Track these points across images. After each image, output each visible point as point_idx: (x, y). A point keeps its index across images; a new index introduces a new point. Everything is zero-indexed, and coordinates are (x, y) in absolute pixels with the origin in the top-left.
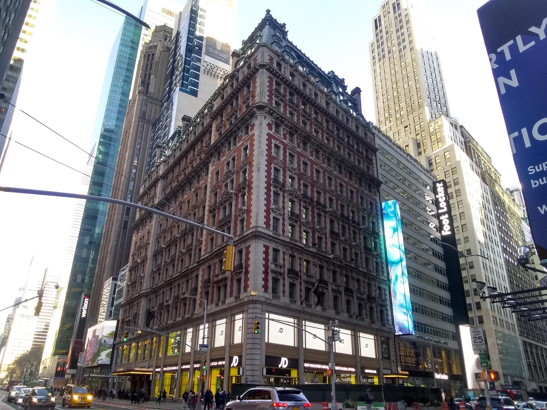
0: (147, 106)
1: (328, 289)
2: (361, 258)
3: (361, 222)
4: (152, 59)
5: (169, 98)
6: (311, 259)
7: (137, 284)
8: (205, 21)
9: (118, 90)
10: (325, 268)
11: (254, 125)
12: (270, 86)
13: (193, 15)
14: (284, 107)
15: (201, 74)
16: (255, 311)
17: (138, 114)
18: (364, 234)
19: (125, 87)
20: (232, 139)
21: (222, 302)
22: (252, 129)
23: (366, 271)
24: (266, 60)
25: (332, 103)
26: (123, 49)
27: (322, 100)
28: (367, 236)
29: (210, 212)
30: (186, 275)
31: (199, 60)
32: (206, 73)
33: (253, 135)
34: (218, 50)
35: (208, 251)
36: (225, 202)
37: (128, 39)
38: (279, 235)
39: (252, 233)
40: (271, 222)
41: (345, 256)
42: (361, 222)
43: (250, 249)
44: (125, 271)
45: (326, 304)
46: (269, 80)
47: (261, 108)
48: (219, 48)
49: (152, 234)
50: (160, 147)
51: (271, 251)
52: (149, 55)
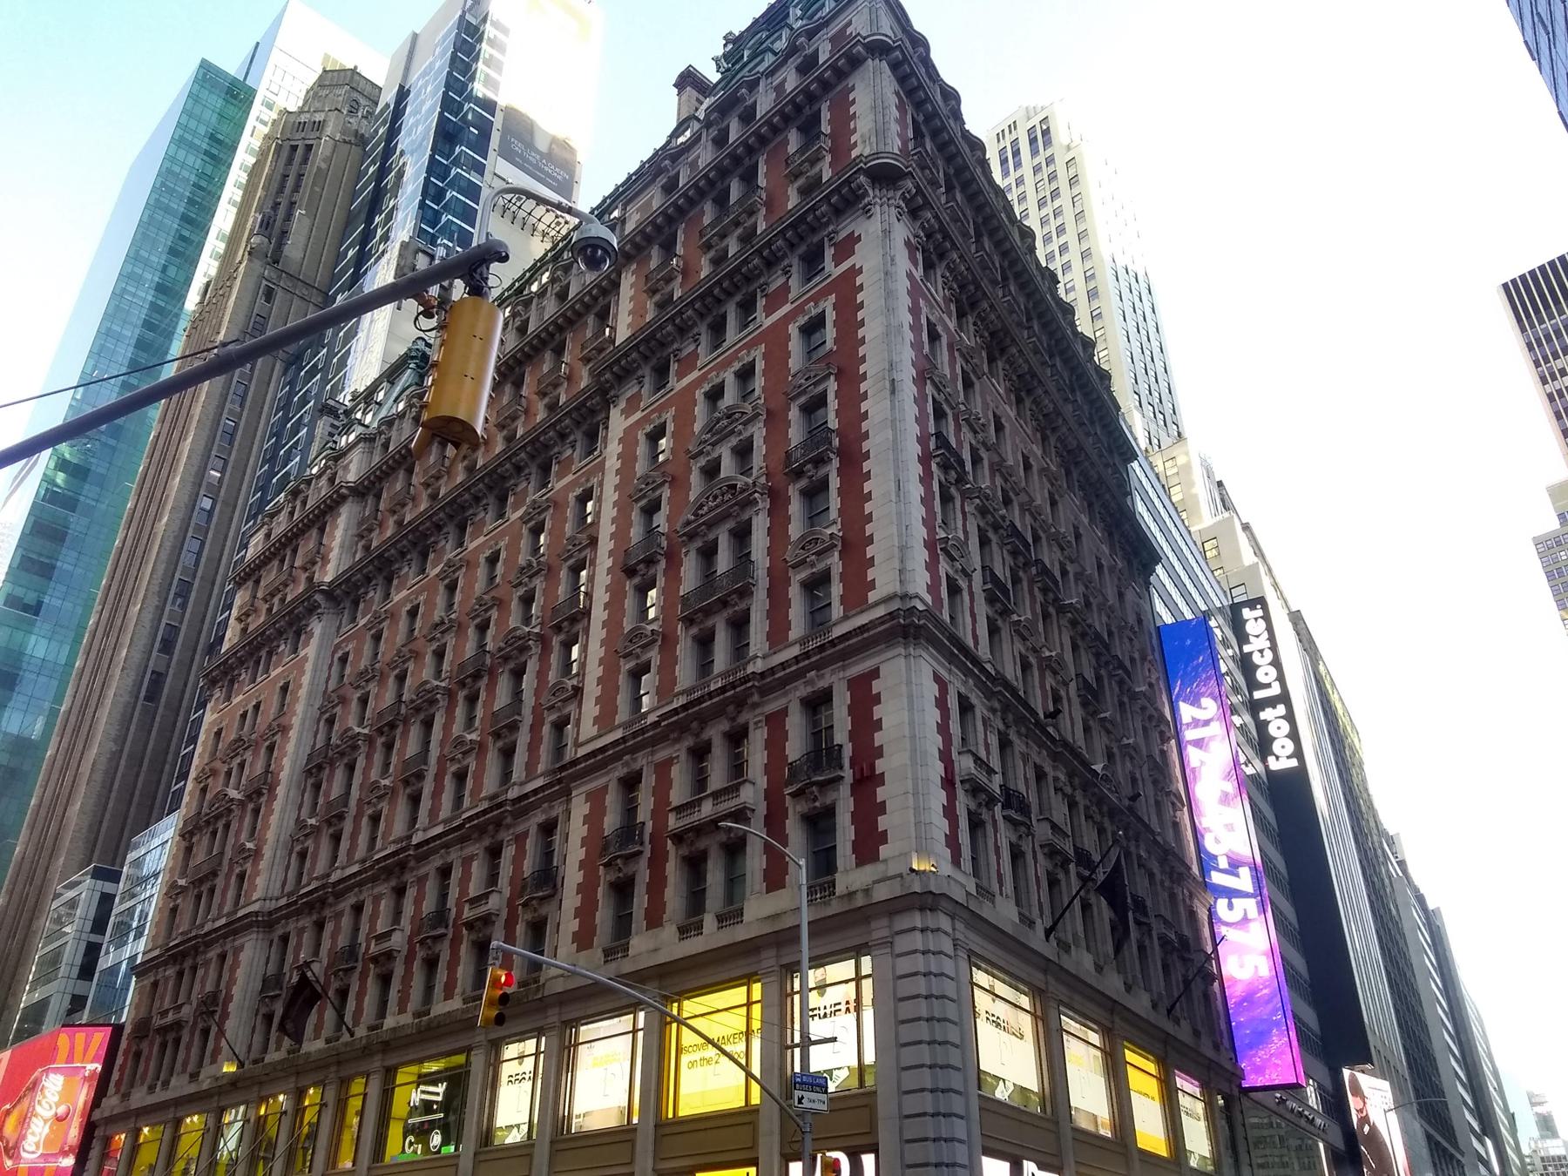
4: (305, 161)
7: (220, 882)
8: (506, 60)
11: (853, 239)
13: (467, 42)
17: (241, 317)
19: (172, 271)
21: (720, 918)
26: (181, 155)
30: (488, 829)
31: (480, 169)
34: (538, 152)
37: (202, 130)
44: (157, 850)
48: (542, 146)
49: (303, 693)
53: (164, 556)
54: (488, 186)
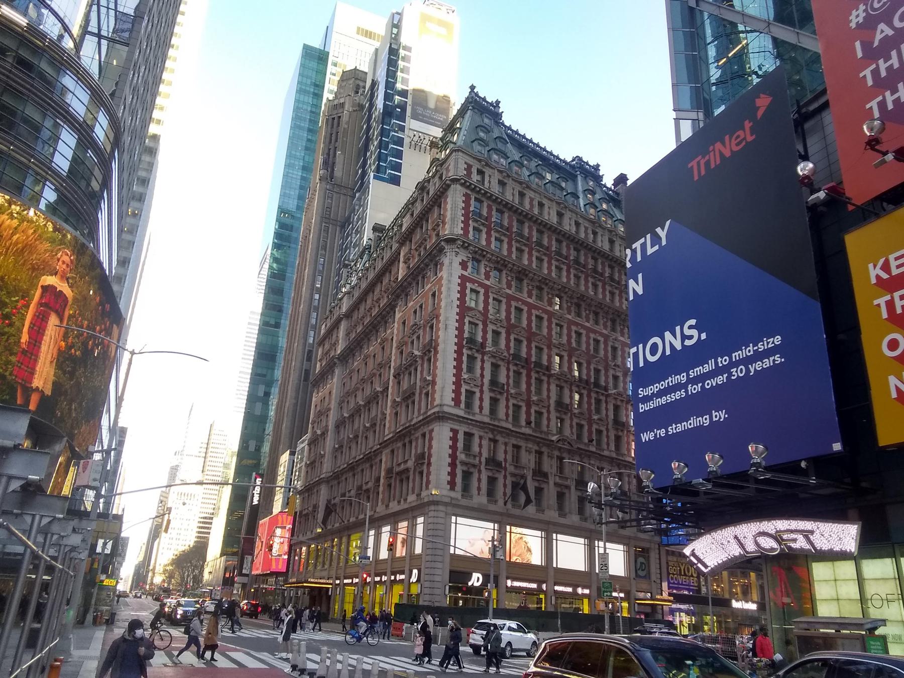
0: (332, 198)
1: (548, 483)
2: (608, 437)
3: (611, 385)
5: (362, 186)
6: (522, 443)
9: (297, 163)
10: (546, 454)
11: (442, 264)
12: (466, 208)
14: (486, 233)
15: (405, 149)
16: (435, 514)
18: (613, 402)
20: (420, 278)
22: (441, 270)
23: (614, 455)
24: (462, 172)
25: (569, 213)
27: (551, 212)
28: (619, 403)
29: (395, 377)
31: (402, 129)
32: (413, 147)
33: (442, 277)
34: (430, 109)
35: (393, 429)
36: (410, 366)
38: (474, 414)
39: (434, 413)
40: (463, 398)
41: (579, 436)
42: (611, 385)
43: (434, 434)
44: (303, 445)
45: (545, 503)
46: (464, 199)
47: (451, 241)
48: (432, 105)
49: (334, 396)
50: (346, 266)
51: (461, 436)
52: (334, 119)
53: (303, 322)
54: (407, 137)
